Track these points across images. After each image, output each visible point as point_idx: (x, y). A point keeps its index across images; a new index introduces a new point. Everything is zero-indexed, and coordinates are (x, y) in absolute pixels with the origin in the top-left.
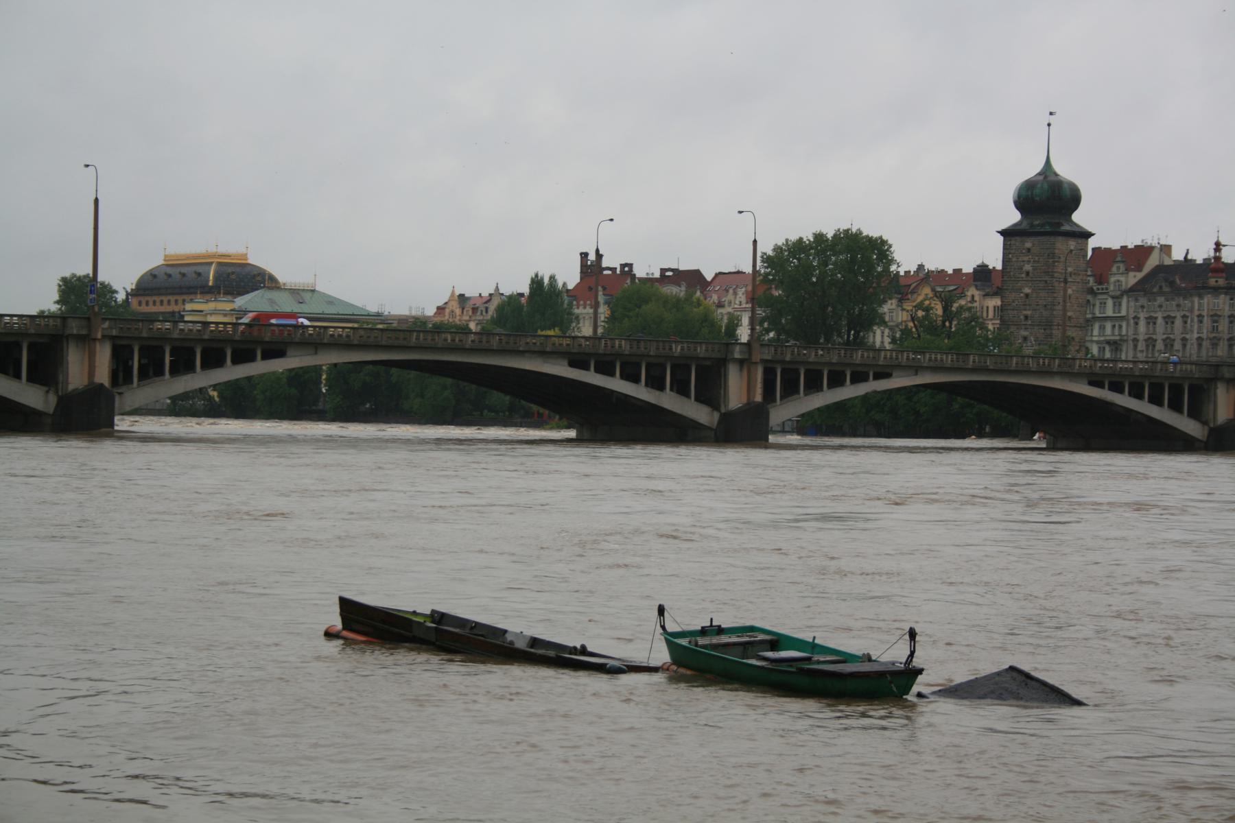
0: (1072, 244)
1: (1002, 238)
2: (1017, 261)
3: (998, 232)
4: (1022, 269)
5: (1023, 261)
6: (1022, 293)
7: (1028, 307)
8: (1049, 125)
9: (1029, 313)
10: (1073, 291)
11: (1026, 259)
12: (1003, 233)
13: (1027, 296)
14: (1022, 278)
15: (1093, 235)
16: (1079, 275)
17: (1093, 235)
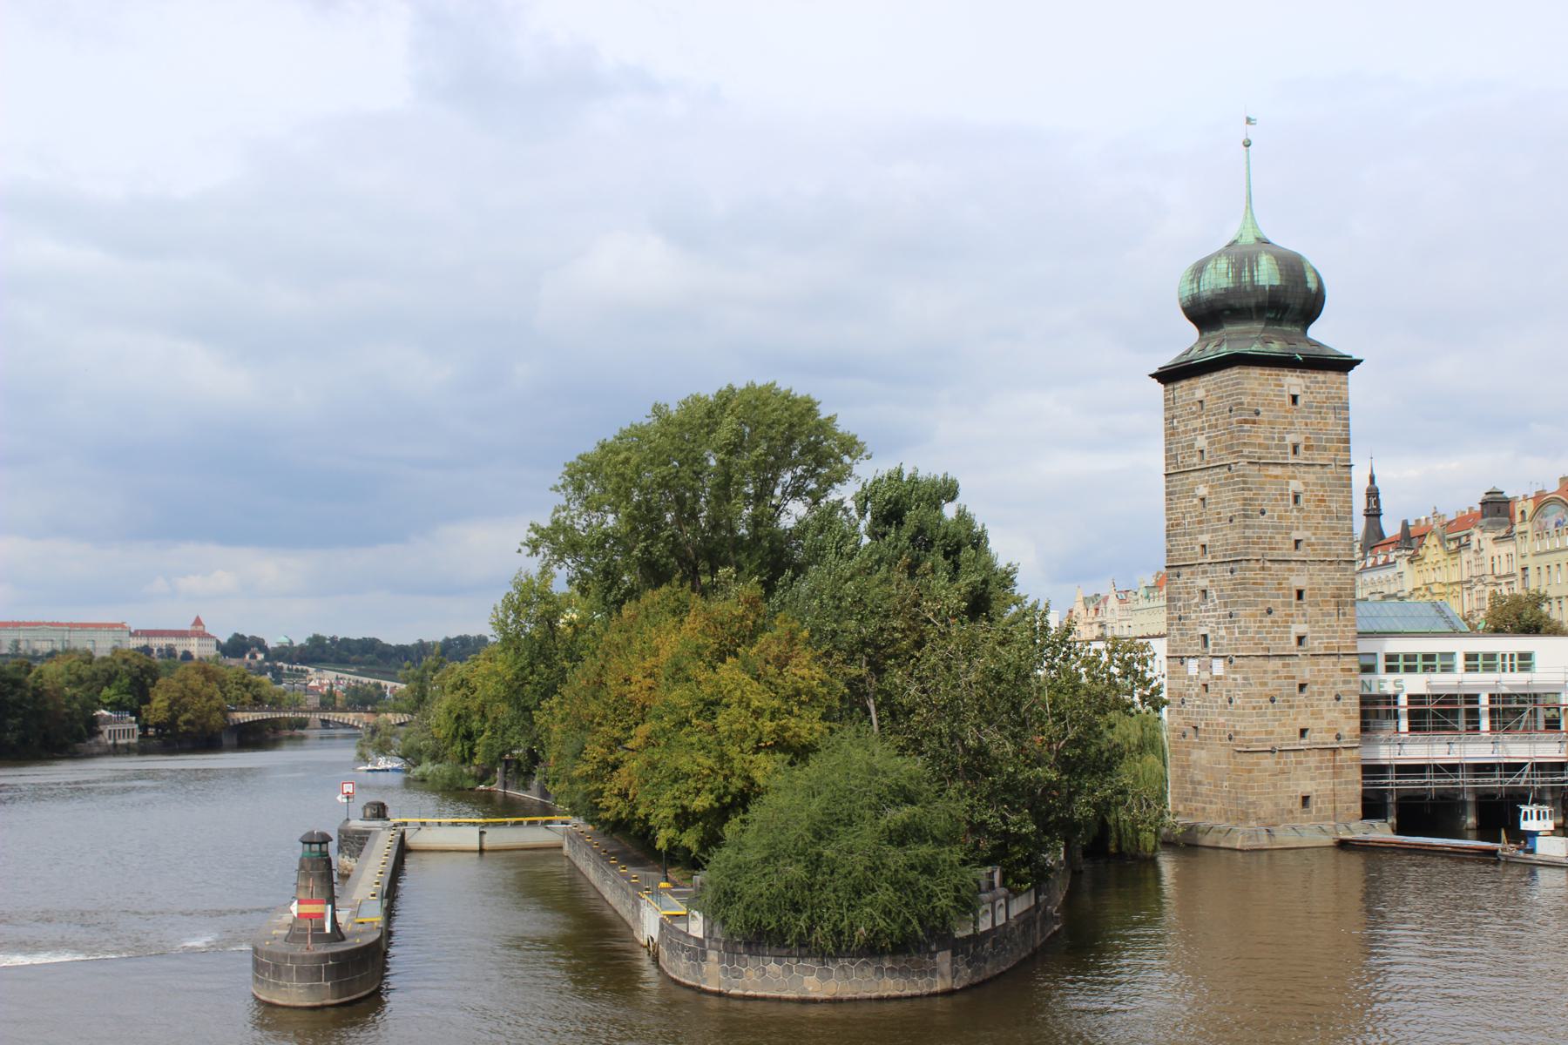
0: (1294, 381)
1: (1161, 386)
2: (1185, 432)
3: (1153, 376)
4: (1192, 446)
5: (1195, 430)
6: (1195, 496)
7: (1205, 527)
8: (1247, 144)
9: (1205, 538)
10: (1306, 484)
11: (1197, 423)
12: (1167, 376)
13: (1203, 499)
14: (1195, 465)
15: (1358, 362)
16: (1325, 449)
17: (1358, 362)
